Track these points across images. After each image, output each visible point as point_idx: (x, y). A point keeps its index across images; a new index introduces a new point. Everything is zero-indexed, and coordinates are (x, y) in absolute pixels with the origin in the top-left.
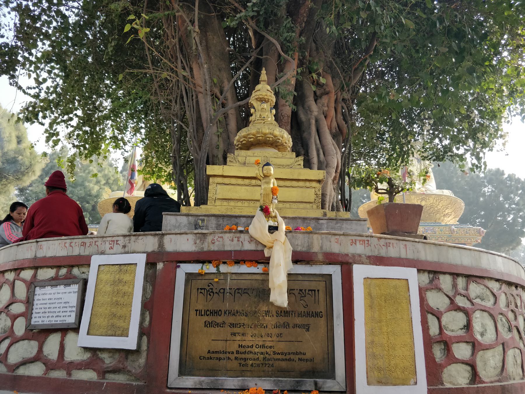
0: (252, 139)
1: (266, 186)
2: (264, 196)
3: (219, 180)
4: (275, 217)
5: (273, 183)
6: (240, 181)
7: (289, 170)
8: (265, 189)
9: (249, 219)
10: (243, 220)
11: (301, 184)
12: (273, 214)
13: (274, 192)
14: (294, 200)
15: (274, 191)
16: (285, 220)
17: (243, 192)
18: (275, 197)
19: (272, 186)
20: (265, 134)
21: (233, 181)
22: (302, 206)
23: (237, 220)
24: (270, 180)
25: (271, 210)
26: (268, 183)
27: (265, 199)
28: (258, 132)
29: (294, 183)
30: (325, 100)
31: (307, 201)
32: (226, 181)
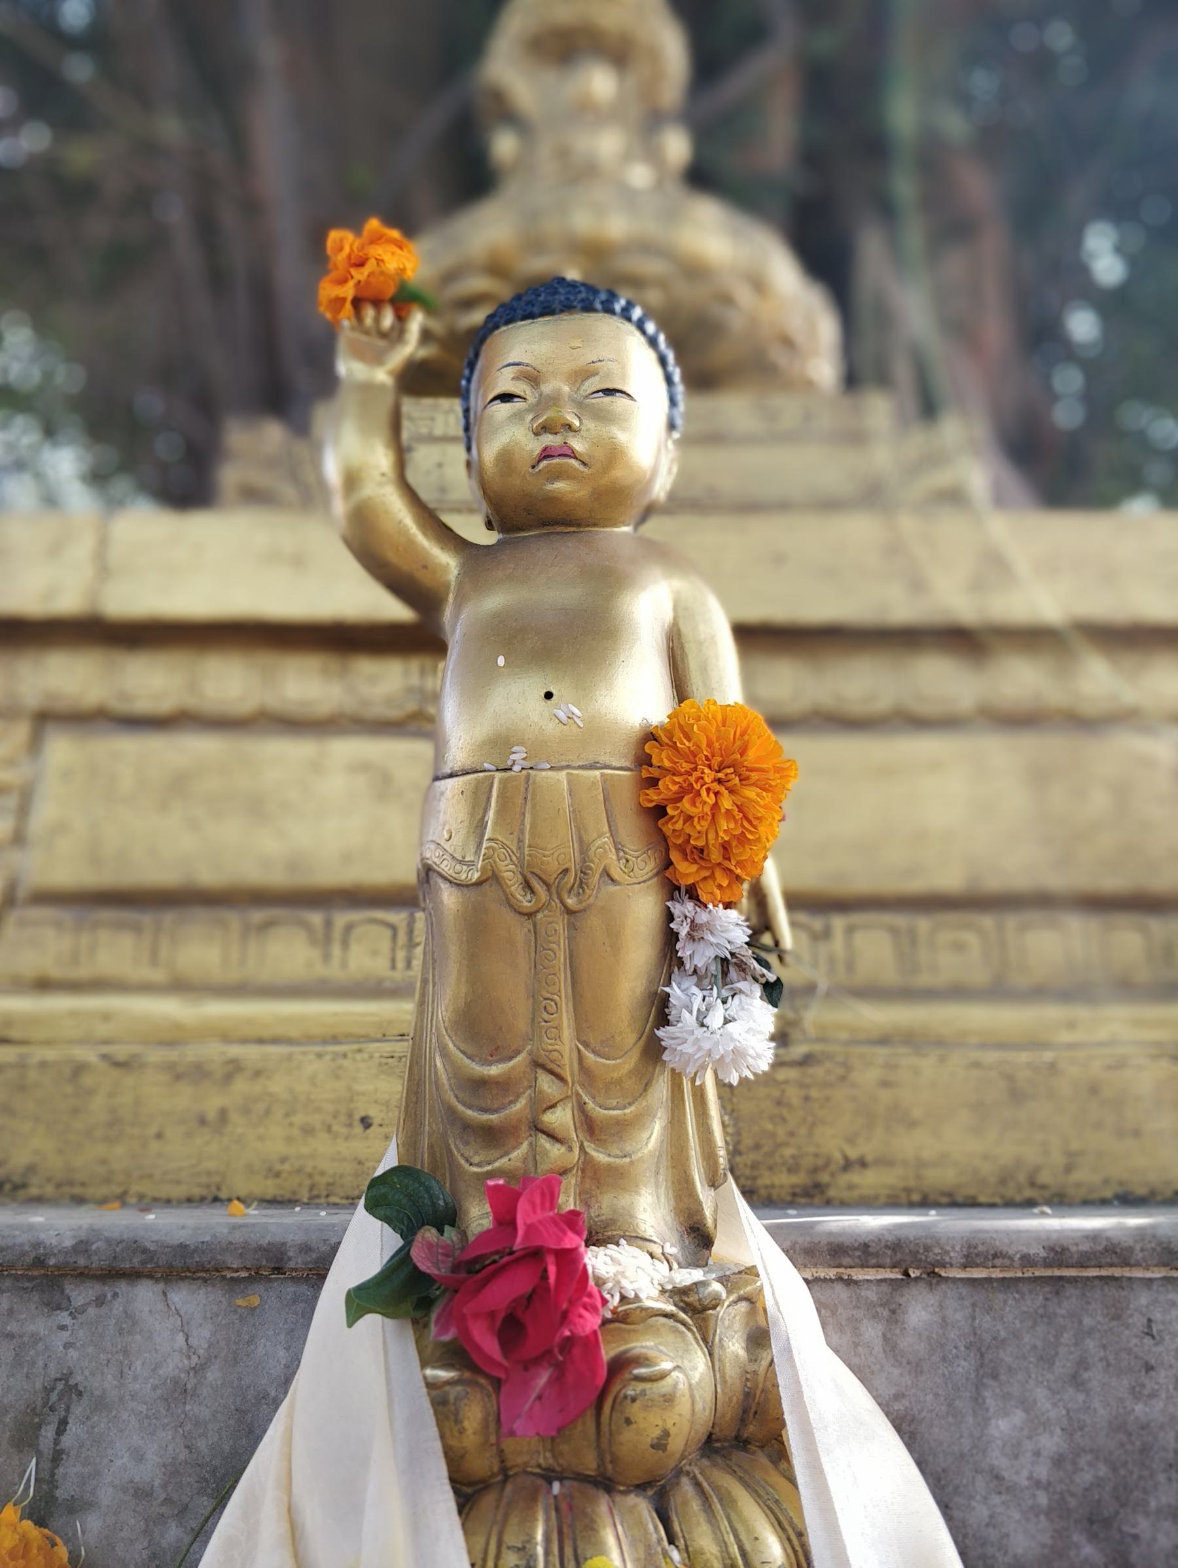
1: (519, 701)
2: (476, 928)
3: (70, 676)
4: (751, 1434)
5: (661, 648)
6: (304, 683)
7: (860, 530)
8: (504, 781)
12: (685, 1377)
13: (694, 817)
15: (685, 805)
16: (920, 1310)
18: (731, 927)
19: (636, 695)
21: (228, 681)
23: (60, 1338)
24: (609, 581)
27: (512, 990)
28: (535, 244)
32: (151, 680)
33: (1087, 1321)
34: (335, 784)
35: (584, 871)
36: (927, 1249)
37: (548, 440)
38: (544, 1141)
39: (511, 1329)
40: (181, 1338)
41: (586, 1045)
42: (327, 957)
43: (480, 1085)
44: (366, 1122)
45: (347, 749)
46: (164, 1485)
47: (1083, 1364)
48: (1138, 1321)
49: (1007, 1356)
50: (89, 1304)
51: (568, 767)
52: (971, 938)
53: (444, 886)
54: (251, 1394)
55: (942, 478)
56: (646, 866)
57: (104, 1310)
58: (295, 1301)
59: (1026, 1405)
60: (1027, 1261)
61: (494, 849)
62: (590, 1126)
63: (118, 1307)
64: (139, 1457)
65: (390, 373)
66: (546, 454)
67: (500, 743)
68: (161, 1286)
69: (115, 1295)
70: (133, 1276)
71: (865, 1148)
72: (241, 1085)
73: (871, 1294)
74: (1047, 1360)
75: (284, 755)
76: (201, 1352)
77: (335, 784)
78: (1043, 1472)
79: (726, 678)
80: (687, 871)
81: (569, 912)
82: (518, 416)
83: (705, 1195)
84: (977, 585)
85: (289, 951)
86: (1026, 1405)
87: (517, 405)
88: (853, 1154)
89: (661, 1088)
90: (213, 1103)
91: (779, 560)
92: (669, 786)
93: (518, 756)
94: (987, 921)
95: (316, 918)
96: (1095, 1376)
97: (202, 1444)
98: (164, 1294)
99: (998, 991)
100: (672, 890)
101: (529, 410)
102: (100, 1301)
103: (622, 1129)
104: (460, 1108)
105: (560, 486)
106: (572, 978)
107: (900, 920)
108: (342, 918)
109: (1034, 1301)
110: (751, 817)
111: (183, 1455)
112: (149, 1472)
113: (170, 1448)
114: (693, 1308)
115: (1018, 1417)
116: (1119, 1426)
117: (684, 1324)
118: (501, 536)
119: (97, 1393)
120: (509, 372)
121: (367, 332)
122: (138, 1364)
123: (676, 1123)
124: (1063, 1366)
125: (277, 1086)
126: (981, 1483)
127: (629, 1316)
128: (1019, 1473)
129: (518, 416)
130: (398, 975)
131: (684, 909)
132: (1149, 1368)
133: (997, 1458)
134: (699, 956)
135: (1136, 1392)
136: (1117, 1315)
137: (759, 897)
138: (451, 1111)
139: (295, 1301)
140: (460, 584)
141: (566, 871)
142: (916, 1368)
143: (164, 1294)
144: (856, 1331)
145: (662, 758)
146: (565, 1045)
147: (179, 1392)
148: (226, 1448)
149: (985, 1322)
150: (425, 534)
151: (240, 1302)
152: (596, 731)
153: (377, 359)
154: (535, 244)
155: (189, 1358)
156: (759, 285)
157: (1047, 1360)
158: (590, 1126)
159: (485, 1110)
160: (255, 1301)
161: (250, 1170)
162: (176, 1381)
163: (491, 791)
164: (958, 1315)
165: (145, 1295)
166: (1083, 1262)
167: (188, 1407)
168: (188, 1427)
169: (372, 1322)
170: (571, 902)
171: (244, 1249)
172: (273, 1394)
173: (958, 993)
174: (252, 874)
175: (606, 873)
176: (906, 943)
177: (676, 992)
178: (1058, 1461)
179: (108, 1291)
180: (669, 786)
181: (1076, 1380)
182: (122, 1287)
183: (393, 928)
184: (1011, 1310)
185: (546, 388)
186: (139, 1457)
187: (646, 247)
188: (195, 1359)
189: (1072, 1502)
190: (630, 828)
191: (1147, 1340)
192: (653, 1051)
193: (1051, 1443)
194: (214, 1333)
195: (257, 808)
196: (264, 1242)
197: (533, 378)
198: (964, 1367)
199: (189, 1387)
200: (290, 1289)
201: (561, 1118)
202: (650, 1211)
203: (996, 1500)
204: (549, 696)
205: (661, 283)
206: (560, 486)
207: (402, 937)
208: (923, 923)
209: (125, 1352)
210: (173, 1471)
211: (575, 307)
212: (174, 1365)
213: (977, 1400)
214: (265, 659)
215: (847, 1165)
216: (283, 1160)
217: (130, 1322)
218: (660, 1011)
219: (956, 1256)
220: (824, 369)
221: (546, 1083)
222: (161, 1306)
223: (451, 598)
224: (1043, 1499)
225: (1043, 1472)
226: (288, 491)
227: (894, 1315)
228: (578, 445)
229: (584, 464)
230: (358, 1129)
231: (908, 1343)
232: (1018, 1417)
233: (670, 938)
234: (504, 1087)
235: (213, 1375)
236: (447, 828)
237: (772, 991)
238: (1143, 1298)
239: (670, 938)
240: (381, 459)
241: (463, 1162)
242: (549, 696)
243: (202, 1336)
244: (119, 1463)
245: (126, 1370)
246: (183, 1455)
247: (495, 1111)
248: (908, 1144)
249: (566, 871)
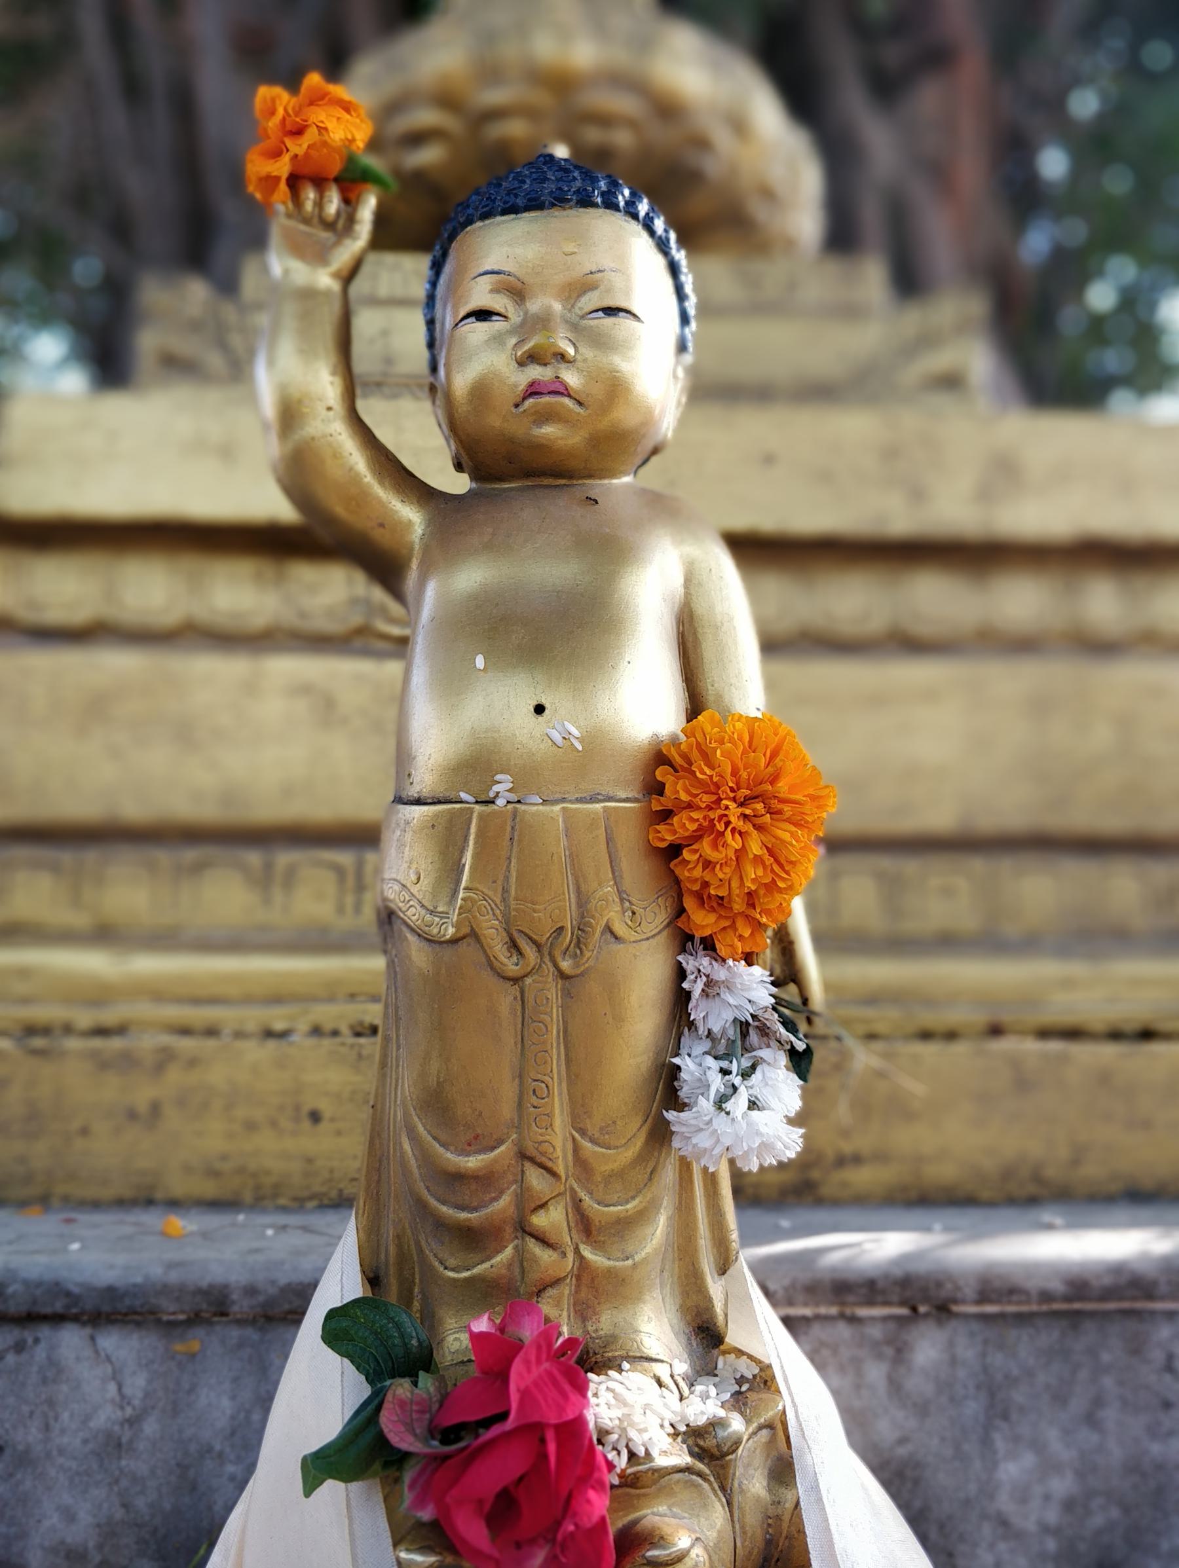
0: (429, 156)
1: (503, 706)
5: (669, 640)
6: (235, 592)
7: (854, 426)
8: (477, 804)
9: (214, 1346)
10: (100, 1376)
11: (1020, 600)
14: (939, 817)
16: (928, 1348)
17: (266, 725)
18: (753, 986)
19: (641, 702)
20: (561, 83)
21: (149, 588)
22: (1039, 890)
24: (610, 552)
25: (641, 1406)
26: (563, 633)
28: (490, 73)
29: (934, 598)
30: (928, 98)
31: (1113, 823)
33: (1106, 1357)
34: (272, 708)
35: (582, 928)
36: (939, 1284)
37: (535, 372)
38: (531, 1243)
39: (503, 1510)
40: (112, 1388)
41: (583, 1132)
42: (267, 901)
43: (458, 1178)
44: (315, 1117)
45: (285, 667)
46: (100, 1547)
47: (1098, 1402)
48: (1158, 1356)
49: (1019, 1396)
50: (7, 1350)
51: (563, 800)
52: (961, 884)
53: (411, 937)
54: (193, 1448)
55: (941, 360)
56: (656, 917)
57: (24, 1357)
58: (241, 1345)
59: (1038, 1447)
60: (1046, 1296)
61: (474, 902)
62: (585, 1226)
63: (40, 1353)
64: (70, 1516)
65: (336, 275)
66: (534, 390)
67: (477, 767)
68: (88, 1331)
69: (37, 1341)
70: (57, 1319)
71: (862, 1142)
72: (174, 1076)
73: (875, 1332)
74: (1060, 1398)
75: (211, 674)
76: (136, 1402)
77: (272, 708)
78: (1052, 1516)
79: (747, 685)
80: (703, 921)
81: (562, 975)
82: (497, 340)
83: (716, 1288)
84: (985, 494)
85: (225, 895)
86: (1038, 1447)
87: (496, 325)
88: (847, 1148)
89: (669, 1174)
90: (143, 1094)
91: (769, 460)
92: (685, 824)
93: (503, 786)
94: (978, 864)
95: (254, 858)
96: (1110, 1415)
97: (140, 1503)
98: (92, 1338)
99: (989, 942)
100: (684, 940)
101: (511, 332)
102: (19, 1347)
103: (625, 1226)
104: (433, 1202)
105: (548, 431)
106: (567, 1055)
107: (886, 863)
108: (284, 858)
109: (1049, 1336)
110: (783, 861)
111: (119, 1514)
112: (82, 1531)
113: (105, 1506)
114: (708, 1449)
115: (1029, 1459)
116: (1133, 1467)
117: (700, 1474)
118: (474, 485)
119: (20, 1448)
120: (485, 283)
121: (307, 221)
122: (65, 1416)
123: (684, 1209)
124: (1078, 1404)
125: (216, 1076)
126: (987, 1530)
127: (640, 1480)
128: (1028, 1520)
129: (497, 340)
130: (347, 922)
131: (697, 963)
132: (1167, 1405)
133: (1004, 1503)
134: (715, 1017)
135: (1154, 1432)
136: (1136, 1349)
137: (785, 944)
138: (421, 1205)
139: (241, 1345)
140: (426, 549)
141: (561, 928)
142: (922, 1409)
143: (92, 1338)
144: (859, 1373)
145: (677, 789)
146: (558, 1138)
147: (112, 1446)
148: (167, 1506)
149: (997, 1359)
150: (381, 483)
151: (179, 1347)
152: (597, 746)
153: (320, 256)
154: (490, 73)
155: (122, 1408)
156: (740, 126)
157: (1060, 1398)
158: (585, 1226)
159: (462, 1208)
160: (195, 1346)
161: (188, 1169)
162: (109, 1435)
163: (469, 828)
164: (967, 1351)
165: (70, 1341)
166: (1107, 1294)
167: (123, 1463)
168: (124, 1483)
169: (332, 1489)
170: (565, 965)
171: (178, 1292)
172: (218, 1447)
173: (947, 943)
174: (182, 807)
175: (608, 929)
176: (892, 888)
177: (688, 1065)
178: (1069, 1505)
179: (28, 1335)
180: (685, 824)
181: (1091, 1420)
182: (44, 1331)
183: (339, 871)
184: (1026, 1346)
185: (534, 306)
186: (70, 1516)
187: (618, 80)
188: (129, 1411)
189: (1082, 1547)
190: (636, 870)
191: (1168, 1378)
192: (660, 1134)
193: (1062, 1485)
194: (150, 1381)
195: (185, 734)
196: (204, 1284)
197: (518, 292)
198: (973, 1408)
199: (124, 1440)
200: (235, 1333)
201: (552, 1219)
202: (656, 1329)
203: (1002, 1546)
204: (539, 709)
205: (631, 123)
206: (548, 431)
207: (351, 881)
208: (910, 866)
209: (51, 1403)
210: (108, 1531)
211: (569, 200)
212: (105, 1417)
213: (986, 1442)
214: (190, 563)
215: (841, 1161)
216: (224, 1157)
217: (54, 1371)
218: (667, 1088)
219: (969, 1292)
220: (805, 220)
221: (536, 1179)
222: (88, 1352)
223: (414, 564)
224: (1051, 1545)
225: (1052, 1516)
226: (215, 361)
227: (900, 1353)
228: (572, 378)
229: (580, 403)
230: (306, 1124)
231: (917, 1385)
232: (1029, 1459)
233: (681, 998)
234: (486, 1181)
235: (150, 1427)
236: (414, 866)
237: (800, 1062)
238: (1165, 1332)
239: (681, 998)
240: (325, 385)
241: (437, 1264)
242: (539, 709)
243: (136, 1384)
244: (47, 1523)
245: (52, 1422)
246: (119, 1514)
247: (475, 1209)
248: (908, 1138)
249: (561, 928)
